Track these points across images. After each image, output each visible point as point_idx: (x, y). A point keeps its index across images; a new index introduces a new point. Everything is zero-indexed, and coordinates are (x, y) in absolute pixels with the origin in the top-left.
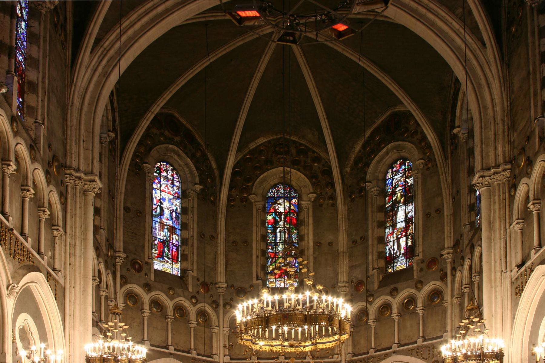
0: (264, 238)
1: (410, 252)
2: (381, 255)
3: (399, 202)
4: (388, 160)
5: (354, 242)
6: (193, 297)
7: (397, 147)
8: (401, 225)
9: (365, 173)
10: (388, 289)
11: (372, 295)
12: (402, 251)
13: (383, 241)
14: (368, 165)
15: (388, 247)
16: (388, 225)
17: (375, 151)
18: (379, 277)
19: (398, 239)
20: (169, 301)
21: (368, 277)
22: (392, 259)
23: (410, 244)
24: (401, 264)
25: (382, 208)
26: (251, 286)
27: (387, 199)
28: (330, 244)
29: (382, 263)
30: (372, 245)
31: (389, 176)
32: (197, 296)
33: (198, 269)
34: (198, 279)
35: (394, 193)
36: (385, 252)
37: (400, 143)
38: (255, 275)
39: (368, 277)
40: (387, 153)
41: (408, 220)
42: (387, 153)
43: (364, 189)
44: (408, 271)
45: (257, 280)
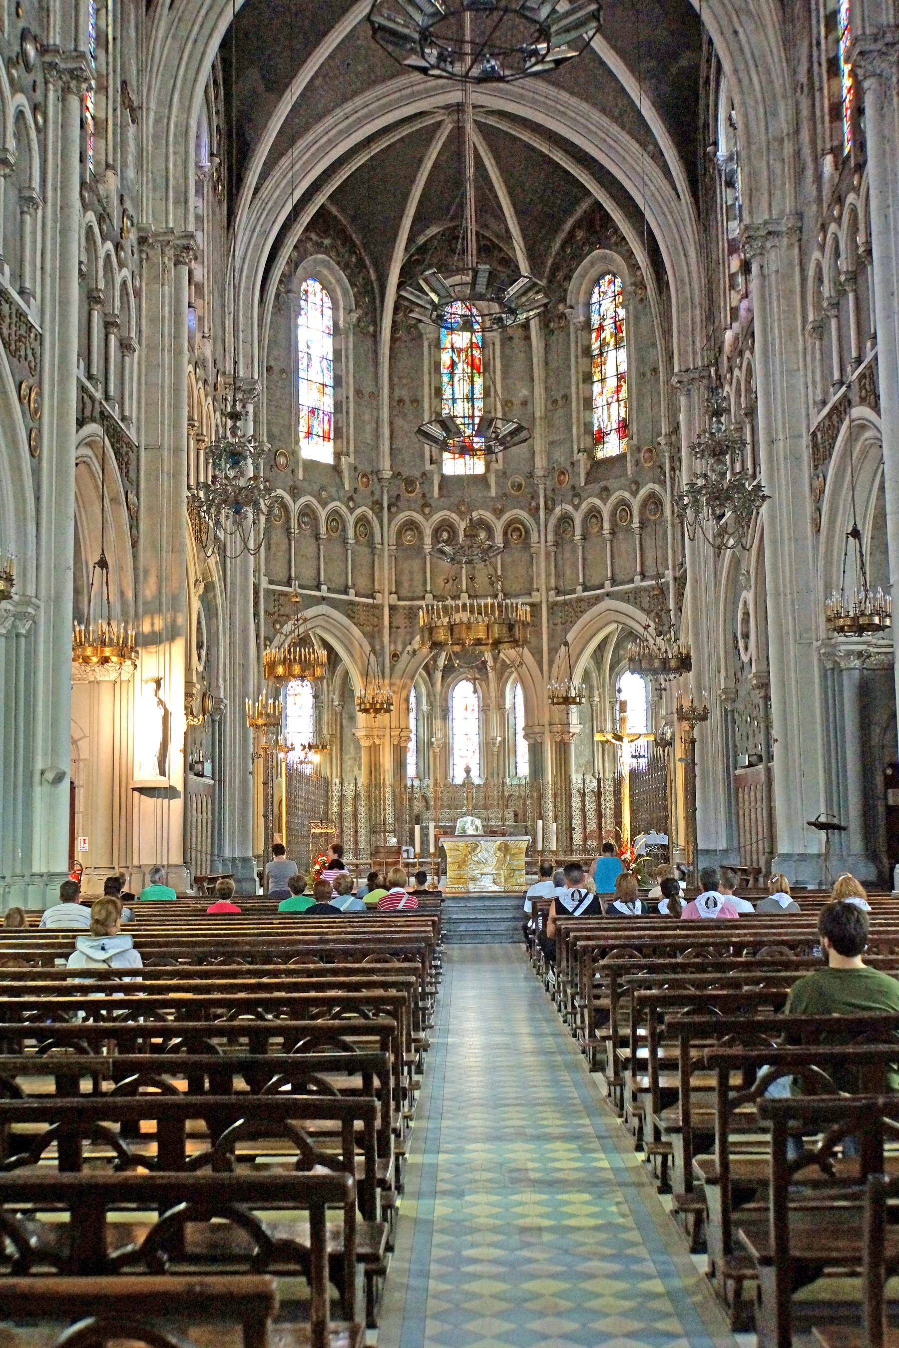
0: (439, 392)
1: (623, 427)
2: (588, 425)
3: (608, 344)
4: (593, 273)
5: (555, 402)
6: (351, 498)
7: (604, 258)
8: (612, 383)
9: (566, 291)
10: (596, 487)
11: (577, 495)
12: (615, 426)
13: (588, 404)
14: (568, 278)
15: (596, 416)
16: (595, 379)
17: (578, 257)
18: (586, 465)
19: (609, 404)
20: (320, 508)
21: (572, 463)
22: (600, 438)
23: (623, 415)
24: (613, 447)
25: (587, 351)
26: (424, 474)
27: (594, 335)
28: (524, 403)
29: (588, 441)
30: (578, 411)
31: (595, 298)
32: (355, 496)
33: (356, 452)
34: (355, 468)
35: (601, 328)
36: (592, 424)
37: (607, 251)
38: (427, 456)
39: (572, 463)
40: (592, 264)
41: (620, 377)
42: (592, 264)
43: (562, 316)
44: (622, 457)
45: (431, 463)
